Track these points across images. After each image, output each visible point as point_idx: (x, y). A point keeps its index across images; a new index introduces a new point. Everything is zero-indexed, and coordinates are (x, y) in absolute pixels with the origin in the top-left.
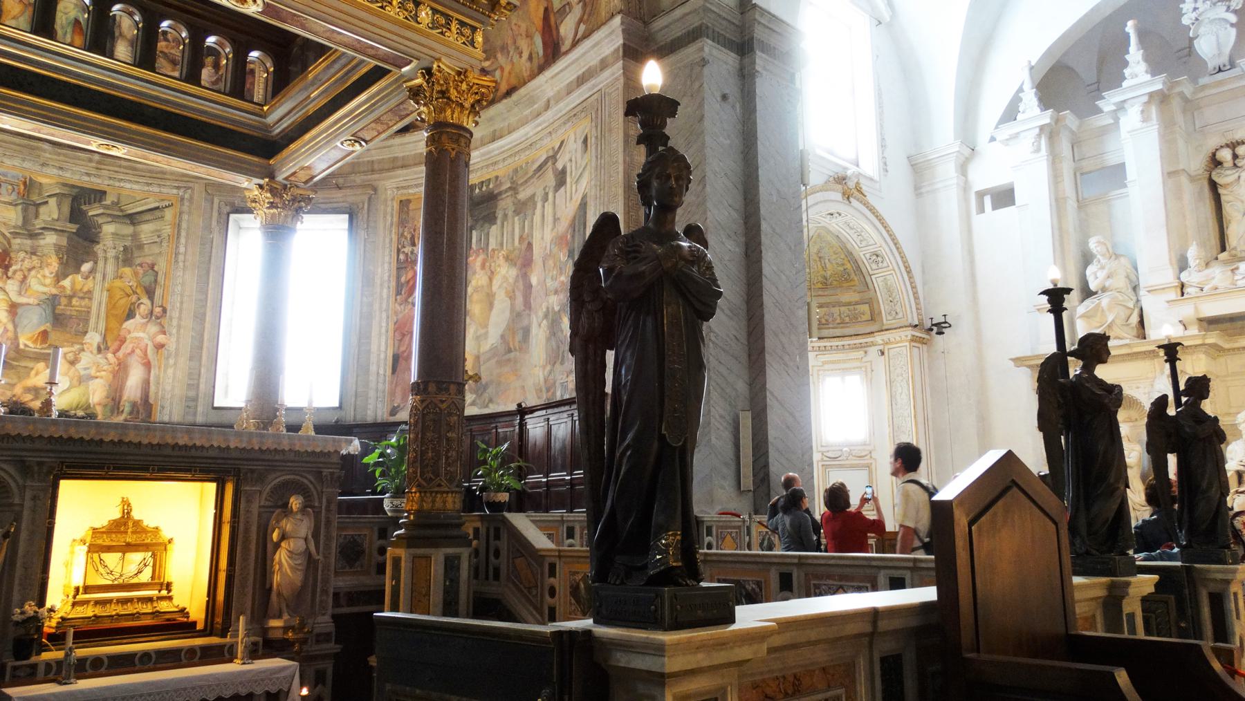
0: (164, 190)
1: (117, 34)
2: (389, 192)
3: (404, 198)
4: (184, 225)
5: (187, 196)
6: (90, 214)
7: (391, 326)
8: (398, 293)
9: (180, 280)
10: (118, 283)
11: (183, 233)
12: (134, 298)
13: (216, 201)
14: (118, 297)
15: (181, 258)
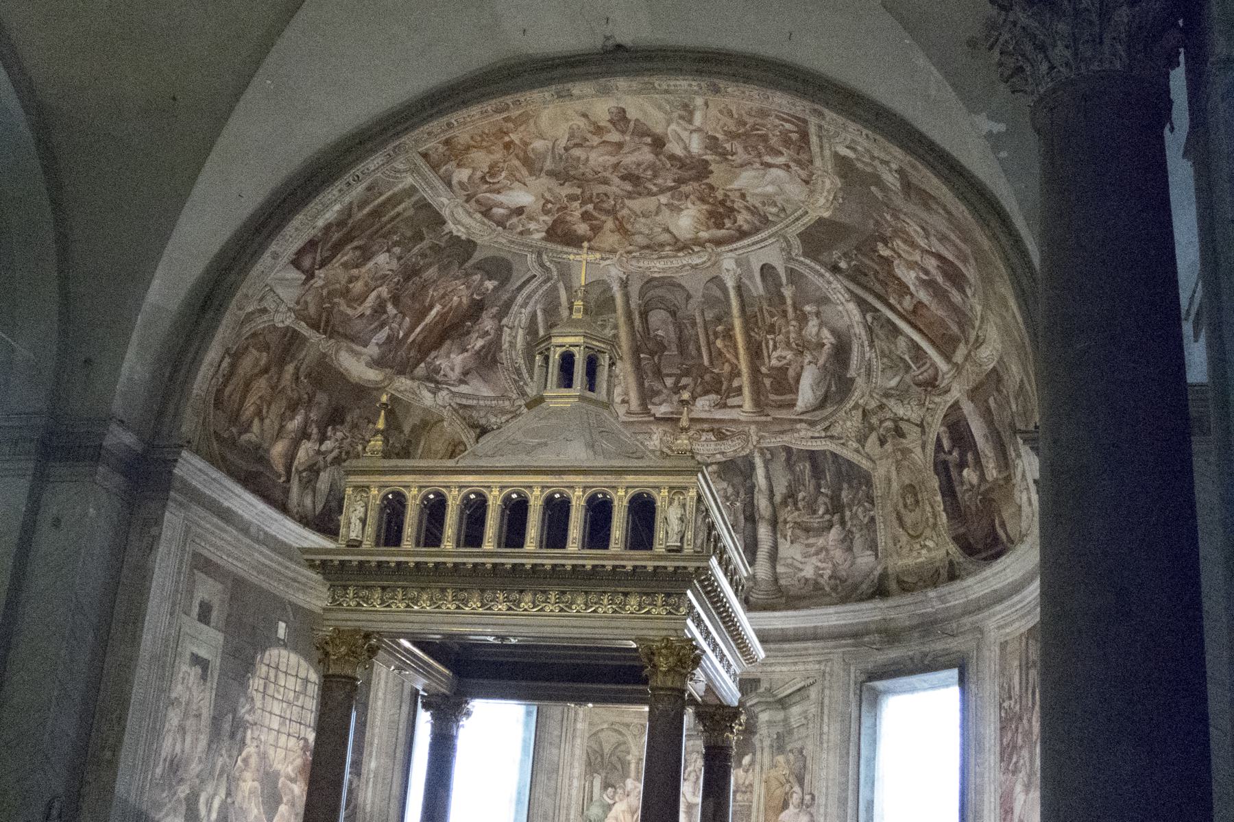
0: (808, 667)
1: (757, 517)
2: (992, 634)
3: (1002, 641)
4: (826, 701)
5: (828, 669)
6: (748, 705)
7: (998, 801)
8: (1002, 760)
9: (824, 764)
10: (773, 773)
11: (826, 711)
12: (787, 787)
13: (852, 669)
14: (774, 786)
15: (825, 737)
